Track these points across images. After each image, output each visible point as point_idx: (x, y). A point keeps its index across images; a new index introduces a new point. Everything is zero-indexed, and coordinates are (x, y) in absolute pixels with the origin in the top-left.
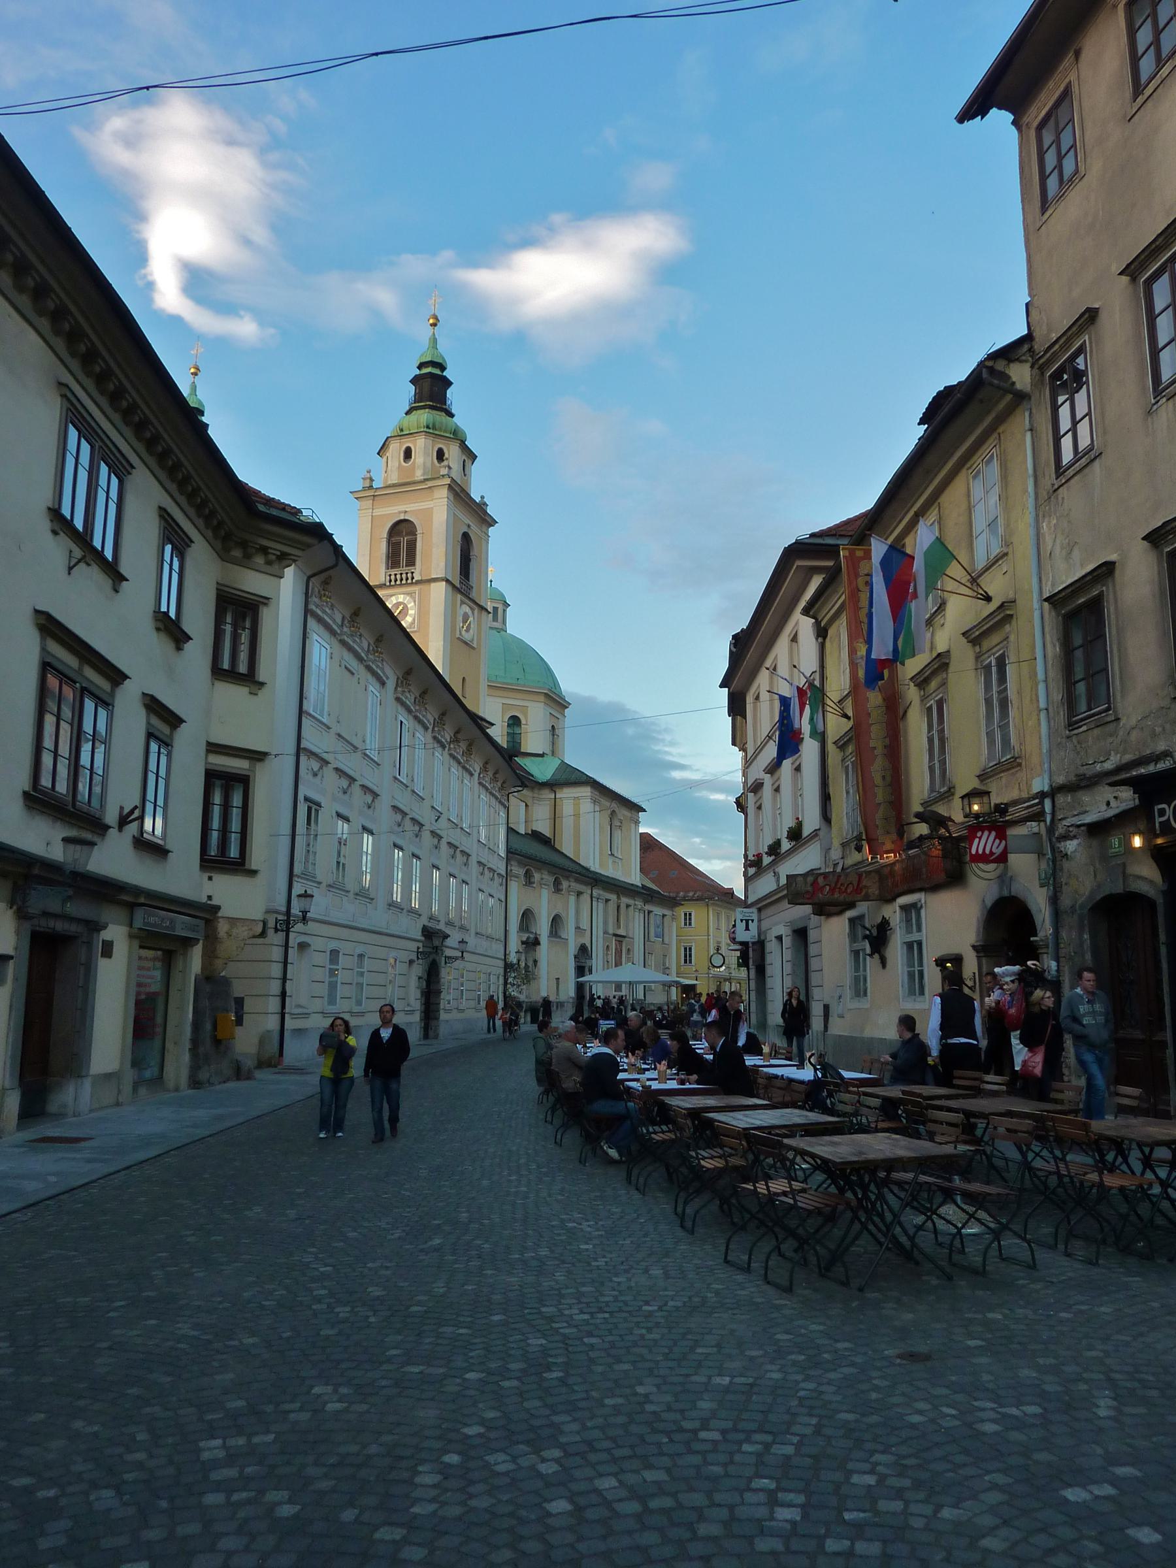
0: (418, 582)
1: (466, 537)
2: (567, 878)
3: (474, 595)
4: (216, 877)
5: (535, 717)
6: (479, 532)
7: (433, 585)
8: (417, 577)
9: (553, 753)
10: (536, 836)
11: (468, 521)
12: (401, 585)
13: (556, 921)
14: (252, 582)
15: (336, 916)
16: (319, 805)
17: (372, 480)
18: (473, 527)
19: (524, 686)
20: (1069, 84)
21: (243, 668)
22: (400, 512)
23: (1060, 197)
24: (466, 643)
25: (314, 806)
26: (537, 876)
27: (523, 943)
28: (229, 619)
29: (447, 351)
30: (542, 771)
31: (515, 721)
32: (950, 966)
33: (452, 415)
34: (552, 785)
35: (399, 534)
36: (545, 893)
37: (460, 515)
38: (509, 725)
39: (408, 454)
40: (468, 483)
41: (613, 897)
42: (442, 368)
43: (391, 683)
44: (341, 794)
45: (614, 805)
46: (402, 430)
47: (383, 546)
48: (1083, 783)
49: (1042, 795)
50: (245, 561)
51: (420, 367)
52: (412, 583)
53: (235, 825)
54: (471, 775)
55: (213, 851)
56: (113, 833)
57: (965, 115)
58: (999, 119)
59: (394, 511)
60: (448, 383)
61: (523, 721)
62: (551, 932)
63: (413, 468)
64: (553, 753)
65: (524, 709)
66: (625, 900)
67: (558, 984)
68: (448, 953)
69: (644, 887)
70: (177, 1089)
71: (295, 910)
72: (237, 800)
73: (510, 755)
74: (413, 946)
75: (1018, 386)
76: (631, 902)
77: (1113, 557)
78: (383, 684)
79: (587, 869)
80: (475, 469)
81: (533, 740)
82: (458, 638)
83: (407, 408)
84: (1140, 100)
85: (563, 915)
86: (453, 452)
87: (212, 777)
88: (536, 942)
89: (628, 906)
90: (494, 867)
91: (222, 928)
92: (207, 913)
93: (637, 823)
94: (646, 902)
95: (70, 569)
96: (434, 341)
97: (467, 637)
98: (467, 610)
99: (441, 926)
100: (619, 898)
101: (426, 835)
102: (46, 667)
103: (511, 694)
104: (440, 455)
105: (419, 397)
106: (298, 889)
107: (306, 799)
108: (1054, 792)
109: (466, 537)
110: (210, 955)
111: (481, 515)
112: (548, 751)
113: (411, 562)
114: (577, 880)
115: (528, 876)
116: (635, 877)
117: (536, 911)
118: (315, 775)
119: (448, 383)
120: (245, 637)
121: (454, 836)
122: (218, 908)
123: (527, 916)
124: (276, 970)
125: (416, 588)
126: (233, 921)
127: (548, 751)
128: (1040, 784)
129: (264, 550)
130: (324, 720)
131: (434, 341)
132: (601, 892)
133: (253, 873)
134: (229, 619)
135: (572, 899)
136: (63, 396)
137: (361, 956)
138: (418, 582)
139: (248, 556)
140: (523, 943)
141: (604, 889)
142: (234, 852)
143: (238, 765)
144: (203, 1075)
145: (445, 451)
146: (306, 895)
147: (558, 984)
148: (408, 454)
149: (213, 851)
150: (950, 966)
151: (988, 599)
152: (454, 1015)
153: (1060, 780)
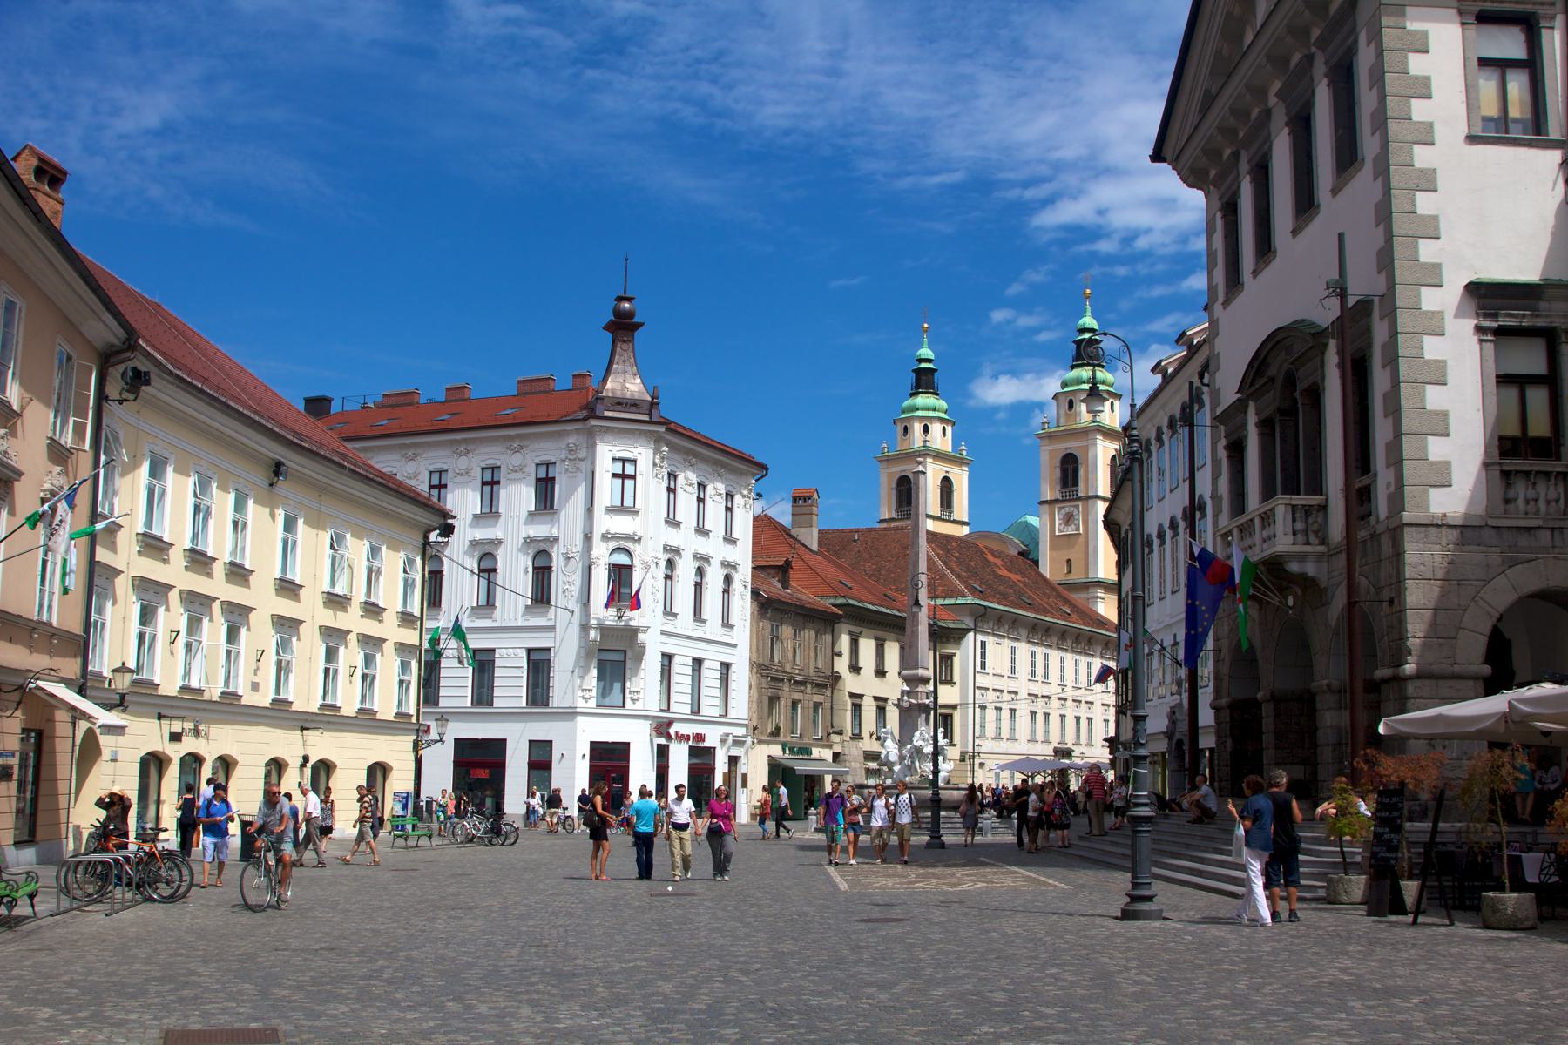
0: (1079, 499)
7: (1090, 501)
8: (1080, 494)
12: (1070, 500)
21: (949, 678)
47: (1058, 473)
99: (1070, 745)
106: (977, 742)
113: (1076, 483)
125: (1080, 504)
133: (955, 745)
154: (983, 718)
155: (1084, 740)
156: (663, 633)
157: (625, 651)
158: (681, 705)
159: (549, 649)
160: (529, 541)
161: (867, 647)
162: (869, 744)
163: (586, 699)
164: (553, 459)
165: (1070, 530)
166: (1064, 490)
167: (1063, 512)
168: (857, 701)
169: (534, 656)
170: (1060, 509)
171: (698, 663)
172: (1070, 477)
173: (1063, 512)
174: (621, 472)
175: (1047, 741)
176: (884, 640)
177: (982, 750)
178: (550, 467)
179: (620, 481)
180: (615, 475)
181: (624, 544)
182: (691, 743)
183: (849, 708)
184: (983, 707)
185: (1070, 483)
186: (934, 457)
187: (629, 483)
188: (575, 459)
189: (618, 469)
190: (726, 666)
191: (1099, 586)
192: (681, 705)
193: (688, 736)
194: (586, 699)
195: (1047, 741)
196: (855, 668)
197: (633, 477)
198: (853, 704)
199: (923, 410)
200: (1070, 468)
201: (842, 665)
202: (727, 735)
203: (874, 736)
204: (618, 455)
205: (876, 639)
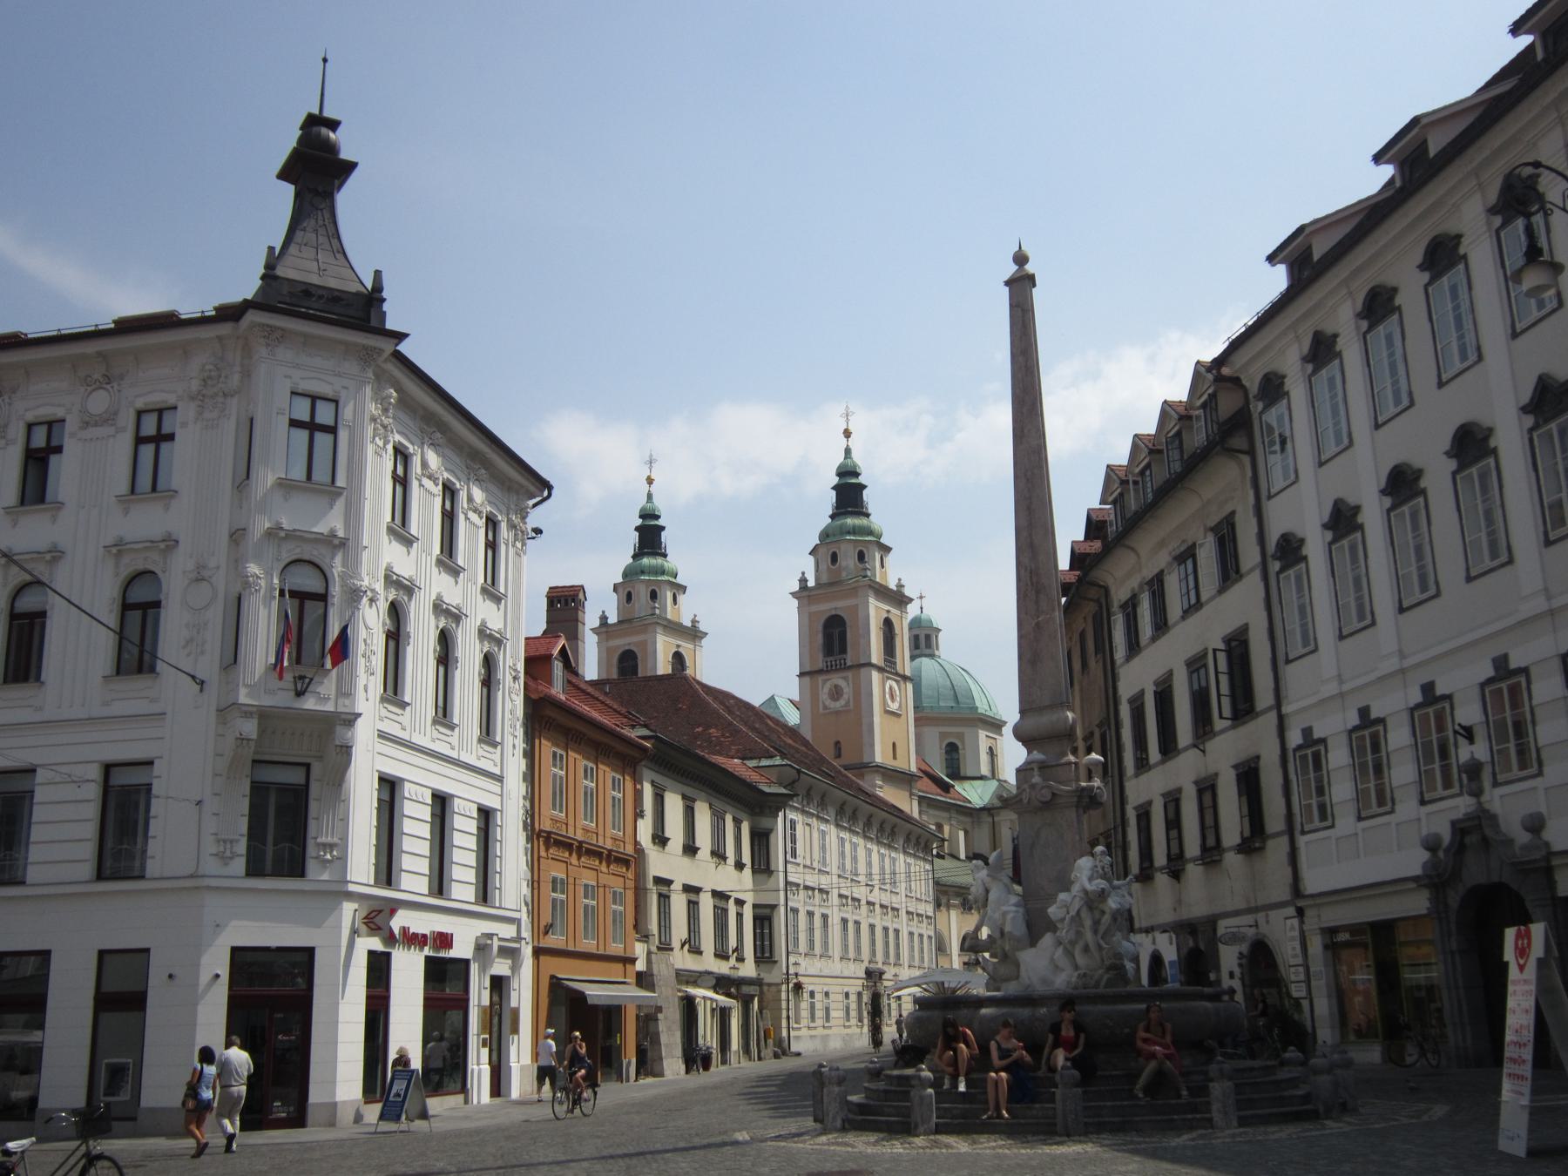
0: (850, 668)
3: (899, 669)
6: (898, 612)
7: (863, 670)
8: (849, 663)
12: (836, 670)
15: (811, 971)
17: (806, 581)
25: (795, 911)
27: (965, 964)
29: (858, 458)
31: (952, 749)
33: (868, 515)
34: (987, 810)
38: (947, 752)
39: (834, 558)
42: (857, 475)
47: (820, 638)
59: (827, 608)
60: (864, 487)
61: (960, 747)
64: (993, 776)
65: (961, 736)
68: (886, 983)
71: (792, 971)
74: (860, 982)
80: (889, 559)
90: (923, 912)
91: (765, 988)
96: (848, 451)
97: (894, 706)
99: (880, 965)
101: (864, 908)
102: (715, 906)
106: (792, 960)
111: (899, 599)
112: (985, 770)
113: (843, 650)
119: (864, 487)
120: (764, 852)
121: (886, 898)
125: (849, 674)
126: (770, 985)
129: (770, 807)
131: (848, 451)
140: (965, 964)
143: (767, 911)
145: (865, 551)
146: (796, 964)
148: (834, 558)
154: (796, 926)
155: (892, 960)
156: (383, 736)
157: (308, 766)
158: (414, 878)
159: (150, 763)
160: (119, 548)
161: (674, 805)
162: (681, 959)
163: (224, 859)
164: (171, 399)
165: (838, 705)
166: (829, 659)
167: (828, 685)
168: (664, 889)
169: (120, 778)
170: (825, 682)
171: (441, 803)
172: (836, 643)
173: (828, 685)
174: (306, 417)
175: (858, 960)
176: (694, 800)
177: (801, 971)
178: (167, 416)
179: (303, 435)
180: (294, 423)
181: (308, 552)
182: (427, 951)
183: (655, 898)
184: (795, 911)
185: (836, 648)
186: (665, 627)
187: (322, 439)
188: (216, 395)
189: (302, 411)
190: (486, 815)
191: (877, 771)
192: (414, 878)
193: (424, 936)
194: (224, 859)
196: (660, 840)
197: (332, 430)
198: (660, 895)
199: (649, 573)
200: (836, 632)
201: (645, 829)
202: (490, 936)
203: (687, 946)
204: (305, 386)
205: (684, 797)
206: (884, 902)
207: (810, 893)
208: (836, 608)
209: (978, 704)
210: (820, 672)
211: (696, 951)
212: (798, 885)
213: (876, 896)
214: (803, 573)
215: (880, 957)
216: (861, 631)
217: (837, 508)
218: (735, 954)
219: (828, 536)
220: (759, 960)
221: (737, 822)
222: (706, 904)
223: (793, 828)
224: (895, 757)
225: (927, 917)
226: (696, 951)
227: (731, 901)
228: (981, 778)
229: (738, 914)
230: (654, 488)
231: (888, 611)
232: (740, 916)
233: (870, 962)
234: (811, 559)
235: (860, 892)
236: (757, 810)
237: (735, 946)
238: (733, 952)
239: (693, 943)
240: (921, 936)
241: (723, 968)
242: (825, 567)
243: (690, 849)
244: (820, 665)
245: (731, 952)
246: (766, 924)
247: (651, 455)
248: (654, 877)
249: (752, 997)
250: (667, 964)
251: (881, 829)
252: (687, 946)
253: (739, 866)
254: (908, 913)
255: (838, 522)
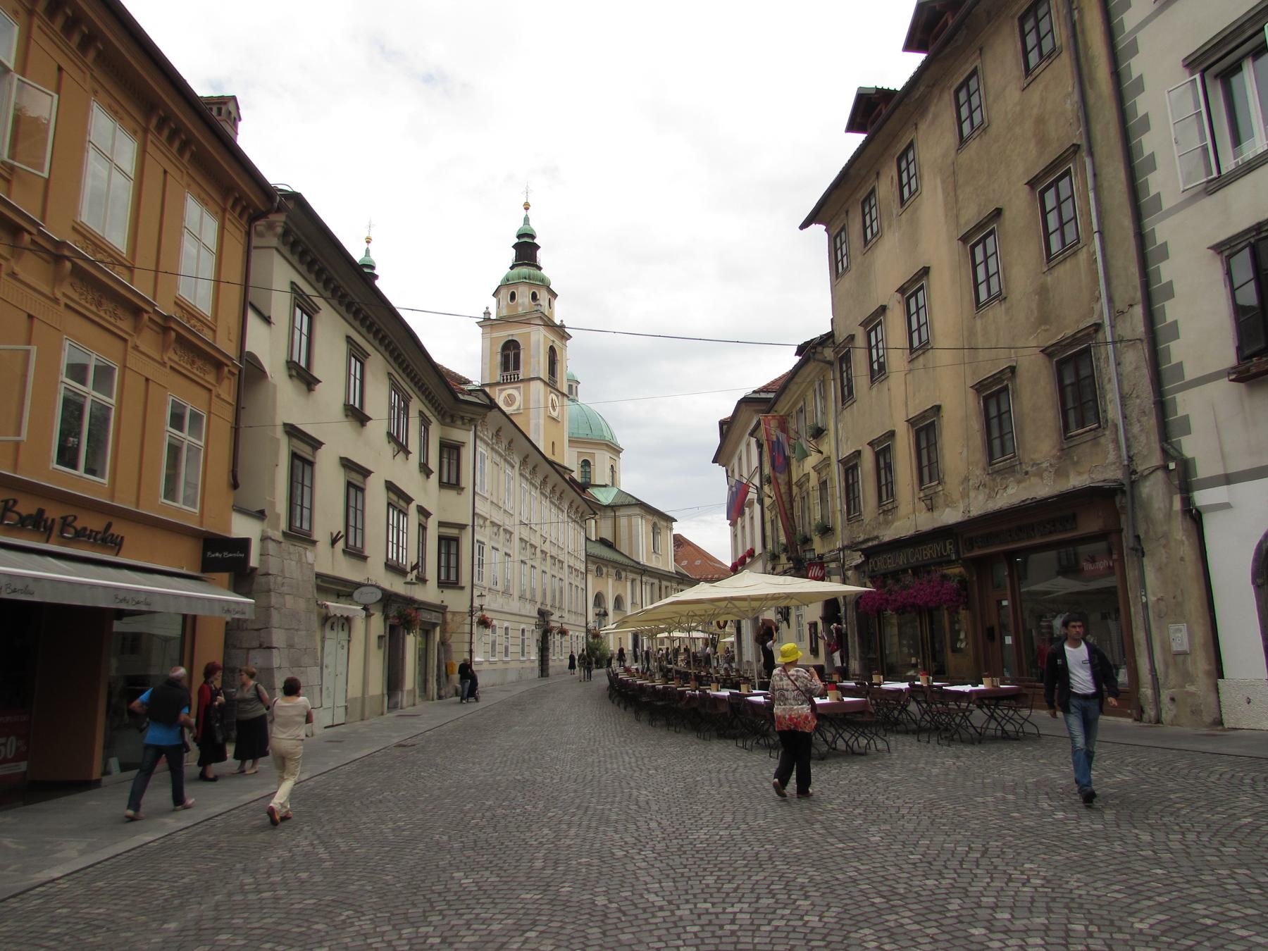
0: (522, 381)
1: (552, 349)
2: (625, 570)
3: (558, 386)
4: (445, 591)
5: (601, 461)
6: (560, 344)
7: (532, 383)
8: (521, 377)
9: (613, 484)
10: (603, 542)
11: (552, 339)
12: (511, 383)
13: (619, 602)
14: (457, 435)
15: (494, 606)
16: (483, 543)
17: (489, 314)
18: (557, 342)
19: (591, 439)
20: (844, 225)
21: (453, 481)
22: (509, 335)
23: (843, 274)
24: (554, 419)
26: (605, 570)
27: (596, 615)
28: (445, 456)
29: (535, 226)
30: (605, 497)
31: (586, 464)
32: (813, 626)
33: (540, 268)
34: (613, 507)
35: (509, 349)
36: (610, 581)
37: (547, 335)
39: (513, 296)
40: (552, 313)
41: (656, 581)
42: (533, 237)
43: (517, 466)
44: (494, 536)
45: (656, 519)
46: (508, 280)
47: (499, 358)
48: (852, 547)
49: (840, 550)
50: (452, 424)
51: (519, 236)
52: (518, 382)
53: (453, 563)
54: (563, 511)
55: (443, 577)
56: (409, 575)
57: (804, 225)
58: (818, 230)
59: (505, 334)
62: (615, 607)
63: (517, 305)
64: (613, 484)
66: (664, 583)
67: (620, 641)
69: (677, 573)
70: (433, 700)
71: (477, 603)
72: (453, 550)
73: (582, 487)
74: (533, 621)
75: (828, 359)
76: (668, 584)
77: (860, 448)
78: (513, 467)
79: (639, 563)
80: (557, 304)
81: (600, 474)
82: (549, 417)
83: (511, 265)
84: (867, 248)
85: (623, 595)
86: (543, 296)
87: (441, 538)
88: (606, 614)
89: (666, 587)
91: (449, 617)
92: (441, 609)
93: (671, 529)
94: (679, 584)
95: (394, 456)
96: (526, 220)
97: (555, 414)
98: (555, 397)
99: (548, 608)
100: (660, 582)
102: (389, 504)
103: (583, 446)
104: (534, 297)
105: (518, 257)
106: (476, 593)
107: (477, 541)
108: (843, 549)
109: (552, 349)
110: (443, 632)
111: (561, 332)
112: (608, 482)
113: (517, 367)
114: (631, 571)
115: (599, 571)
116: (671, 567)
117: (605, 594)
118: (481, 527)
119: (537, 247)
120: (454, 462)
121: (554, 552)
122: (447, 607)
123: (599, 599)
124: (467, 637)
125: (521, 385)
126: (454, 613)
127: (608, 482)
128: (839, 545)
129: (462, 418)
130: (486, 495)
131: (526, 220)
132: (648, 578)
133: (462, 588)
134: (445, 456)
135: (629, 584)
136: (390, 379)
137: (507, 629)
138: (522, 381)
139: (453, 421)
140: (596, 615)
141: (650, 576)
142: (453, 577)
143: (453, 532)
144: (443, 693)
146: (481, 595)
147: (620, 641)
148: (513, 296)
149: (443, 577)
150: (813, 626)
151: (822, 453)
152: (557, 663)
153: (846, 543)
170: (502, 390)
172: (512, 362)
175: (533, 601)
185: (511, 367)
195: (533, 601)
198: (294, 456)
203: (341, 544)
206: (552, 554)
207: (495, 529)
208: (512, 335)
209: (605, 434)
210: (498, 384)
211: (356, 554)
212: (485, 519)
213: (547, 547)
214: (487, 308)
215: (549, 602)
216: (532, 353)
217: (516, 261)
218: (415, 572)
219: (508, 280)
220: (443, 584)
221: (425, 423)
222: (376, 498)
223: (483, 461)
224: (553, 454)
225: (581, 572)
226: (356, 554)
227: (413, 507)
228: (605, 486)
229: (420, 525)
230: (371, 246)
231: (553, 341)
232: (423, 528)
233: (542, 604)
234: (495, 300)
235: (536, 540)
236: (448, 420)
237: (415, 562)
238: (412, 570)
239: (351, 542)
240: (576, 586)
241: (397, 585)
242: (505, 303)
243: (357, 415)
244: (498, 378)
245: (409, 569)
246: (453, 544)
247: (370, 222)
248: (285, 425)
249: (434, 625)
250: (300, 561)
251: (553, 491)
252: (341, 544)
253: (425, 469)
254: (569, 566)
255: (516, 270)
